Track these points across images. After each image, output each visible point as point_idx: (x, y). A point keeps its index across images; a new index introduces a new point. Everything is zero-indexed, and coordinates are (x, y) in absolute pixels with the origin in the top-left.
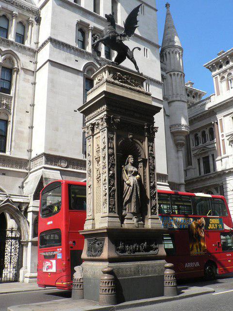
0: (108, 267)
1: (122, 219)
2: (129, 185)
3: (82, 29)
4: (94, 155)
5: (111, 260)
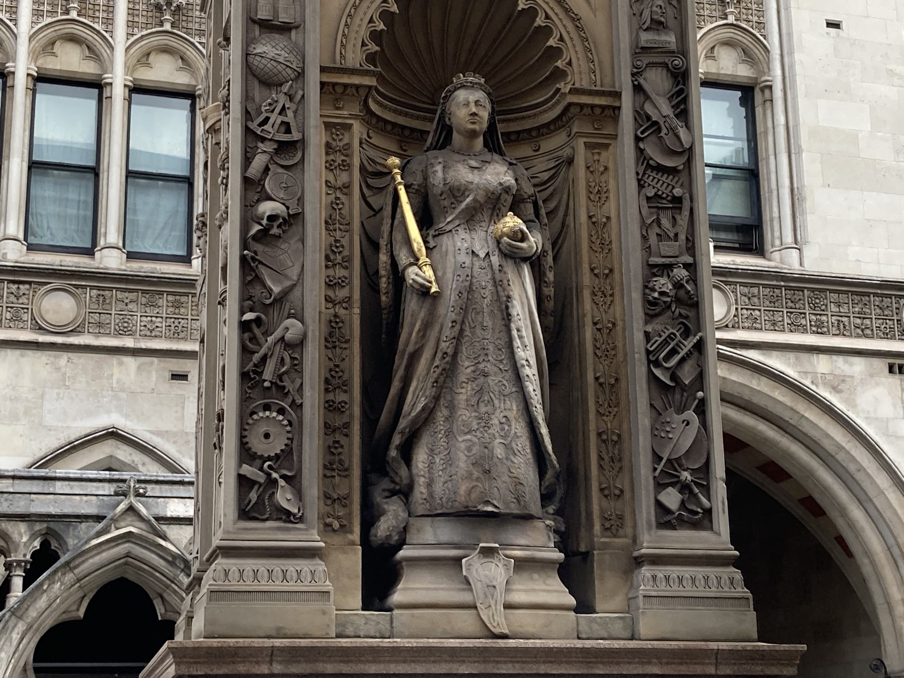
2: (424, 292)
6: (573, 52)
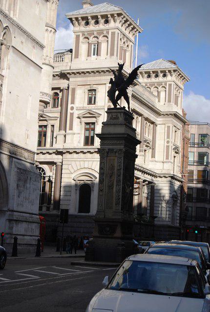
2: (127, 193)
5: (122, 238)
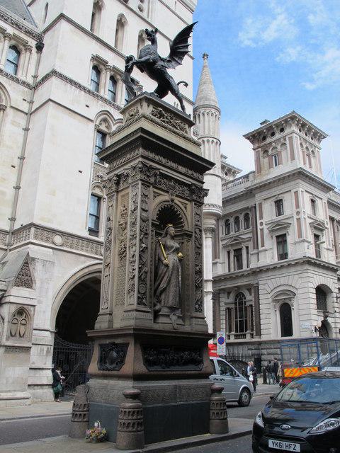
0: (133, 387)
1: (156, 315)
2: (167, 266)
3: (98, 66)
4: (118, 220)
5: (137, 377)
6: (185, 223)
